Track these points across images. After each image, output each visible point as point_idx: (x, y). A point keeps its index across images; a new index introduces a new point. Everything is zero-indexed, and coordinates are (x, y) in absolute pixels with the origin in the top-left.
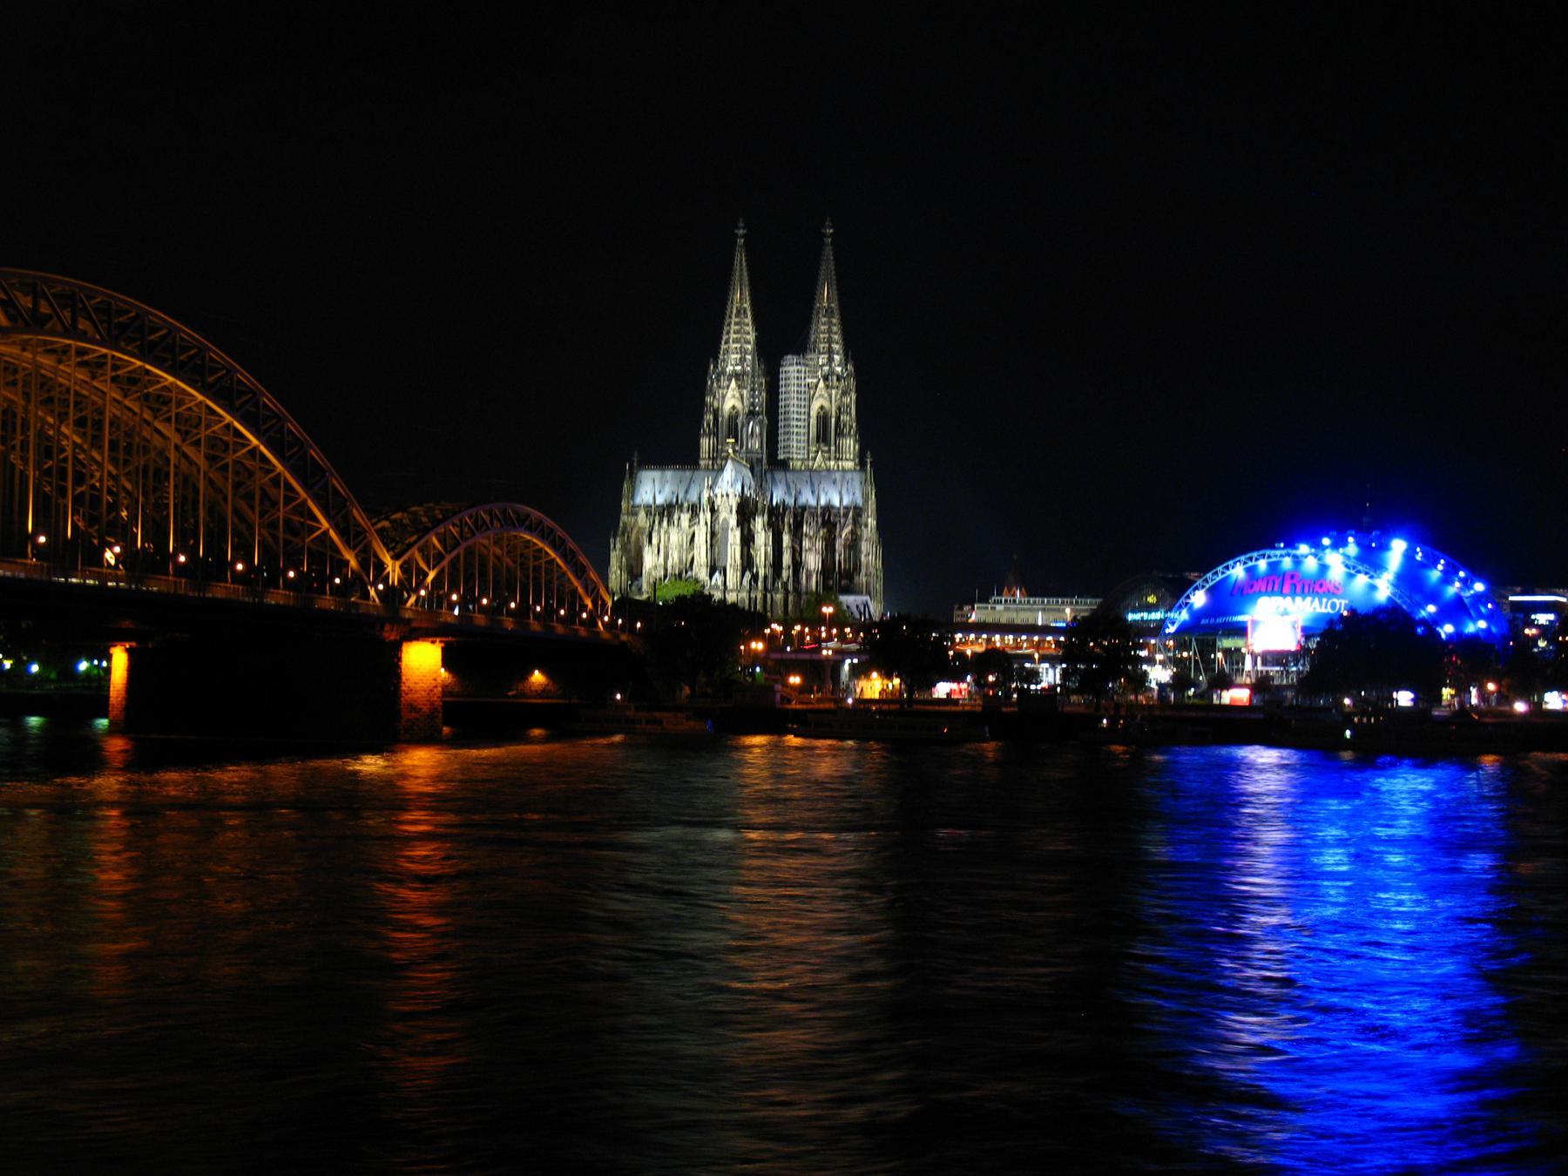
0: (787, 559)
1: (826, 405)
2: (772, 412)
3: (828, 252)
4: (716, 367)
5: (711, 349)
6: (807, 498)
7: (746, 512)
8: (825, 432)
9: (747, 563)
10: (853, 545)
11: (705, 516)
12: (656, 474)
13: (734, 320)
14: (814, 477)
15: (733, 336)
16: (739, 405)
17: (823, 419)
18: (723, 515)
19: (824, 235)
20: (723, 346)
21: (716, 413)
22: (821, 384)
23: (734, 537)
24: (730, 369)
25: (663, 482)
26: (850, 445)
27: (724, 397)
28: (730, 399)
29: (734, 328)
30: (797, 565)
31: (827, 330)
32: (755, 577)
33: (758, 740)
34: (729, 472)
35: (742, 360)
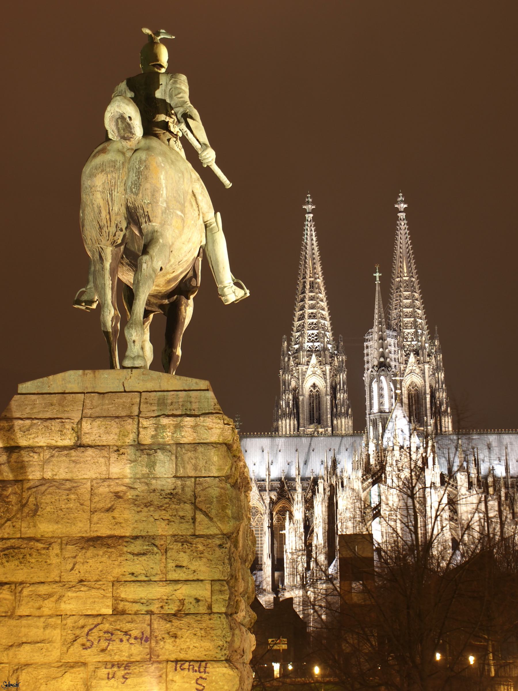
1: (418, 381)
3: (403, 226)
4: (289, 345)
12: (265, 442)
13: (308, 294)
15: (308, 311)
16: (321, 384)
19: (398, 211)
20: (297, 323)
21: (296, 392)
22: (412, 359)
24: (307, 345)
27: (304, 375)
29: (309, 303)
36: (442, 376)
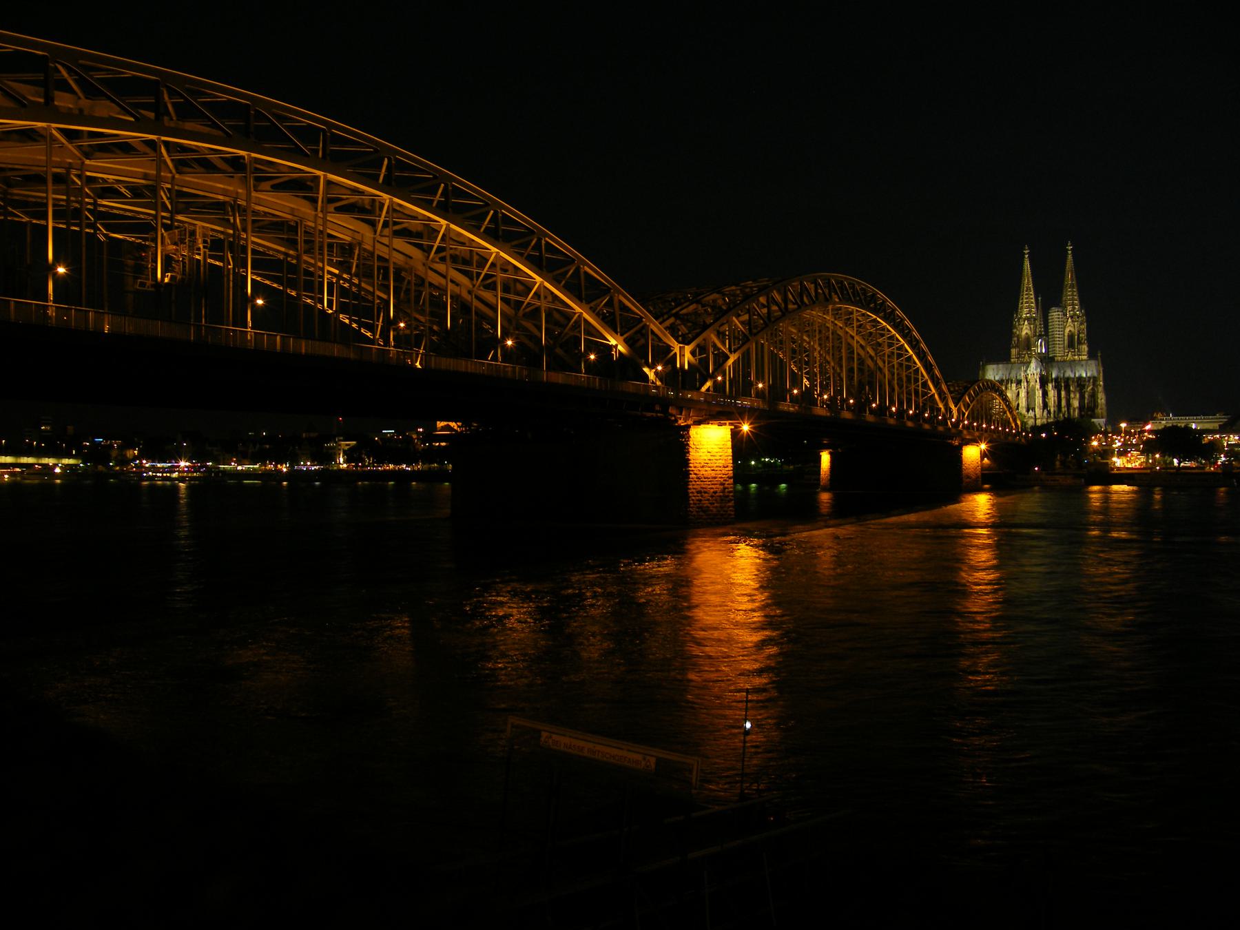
0: (1063, 403)
2: (1045, 334)
3: (1070, 257)
5: (1014, 307)
6: (1069, 374)
7: (1044, 382)
8: (1072, 343)
9: (1045, 405)
10: (1093, 395)
11: (1024, 384)
14: (1072, 364)
17: (1071, 336)
18: (1032, 383)
21: (1018, 337)
23: (1039, 393)
25: (998, 369)
26: (1085, 348)
28: (1025, 330)
30: (1069, 405)
31: (1071, 295)
32: (1049, 412)
33: (1096, 488)
34: (1033, 365)
35: (1030, 312)
36: (1084, 327)
